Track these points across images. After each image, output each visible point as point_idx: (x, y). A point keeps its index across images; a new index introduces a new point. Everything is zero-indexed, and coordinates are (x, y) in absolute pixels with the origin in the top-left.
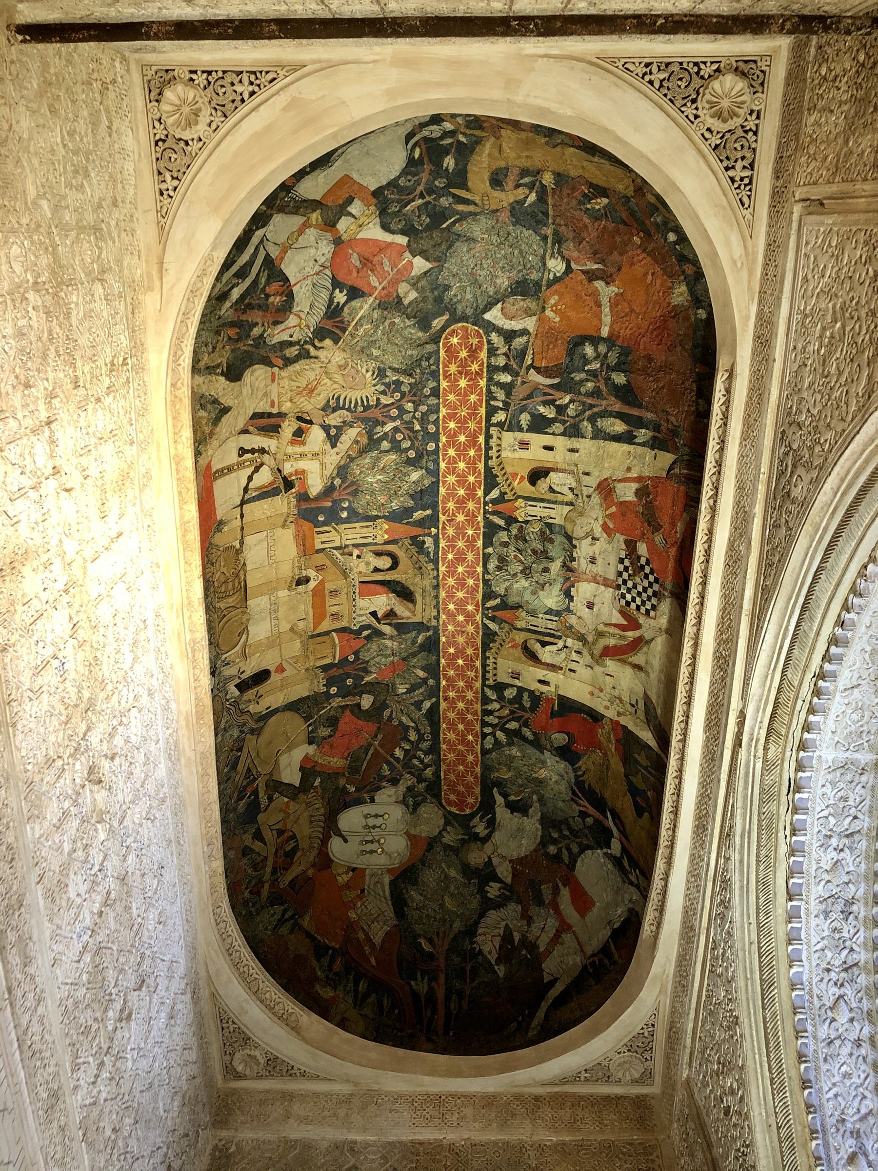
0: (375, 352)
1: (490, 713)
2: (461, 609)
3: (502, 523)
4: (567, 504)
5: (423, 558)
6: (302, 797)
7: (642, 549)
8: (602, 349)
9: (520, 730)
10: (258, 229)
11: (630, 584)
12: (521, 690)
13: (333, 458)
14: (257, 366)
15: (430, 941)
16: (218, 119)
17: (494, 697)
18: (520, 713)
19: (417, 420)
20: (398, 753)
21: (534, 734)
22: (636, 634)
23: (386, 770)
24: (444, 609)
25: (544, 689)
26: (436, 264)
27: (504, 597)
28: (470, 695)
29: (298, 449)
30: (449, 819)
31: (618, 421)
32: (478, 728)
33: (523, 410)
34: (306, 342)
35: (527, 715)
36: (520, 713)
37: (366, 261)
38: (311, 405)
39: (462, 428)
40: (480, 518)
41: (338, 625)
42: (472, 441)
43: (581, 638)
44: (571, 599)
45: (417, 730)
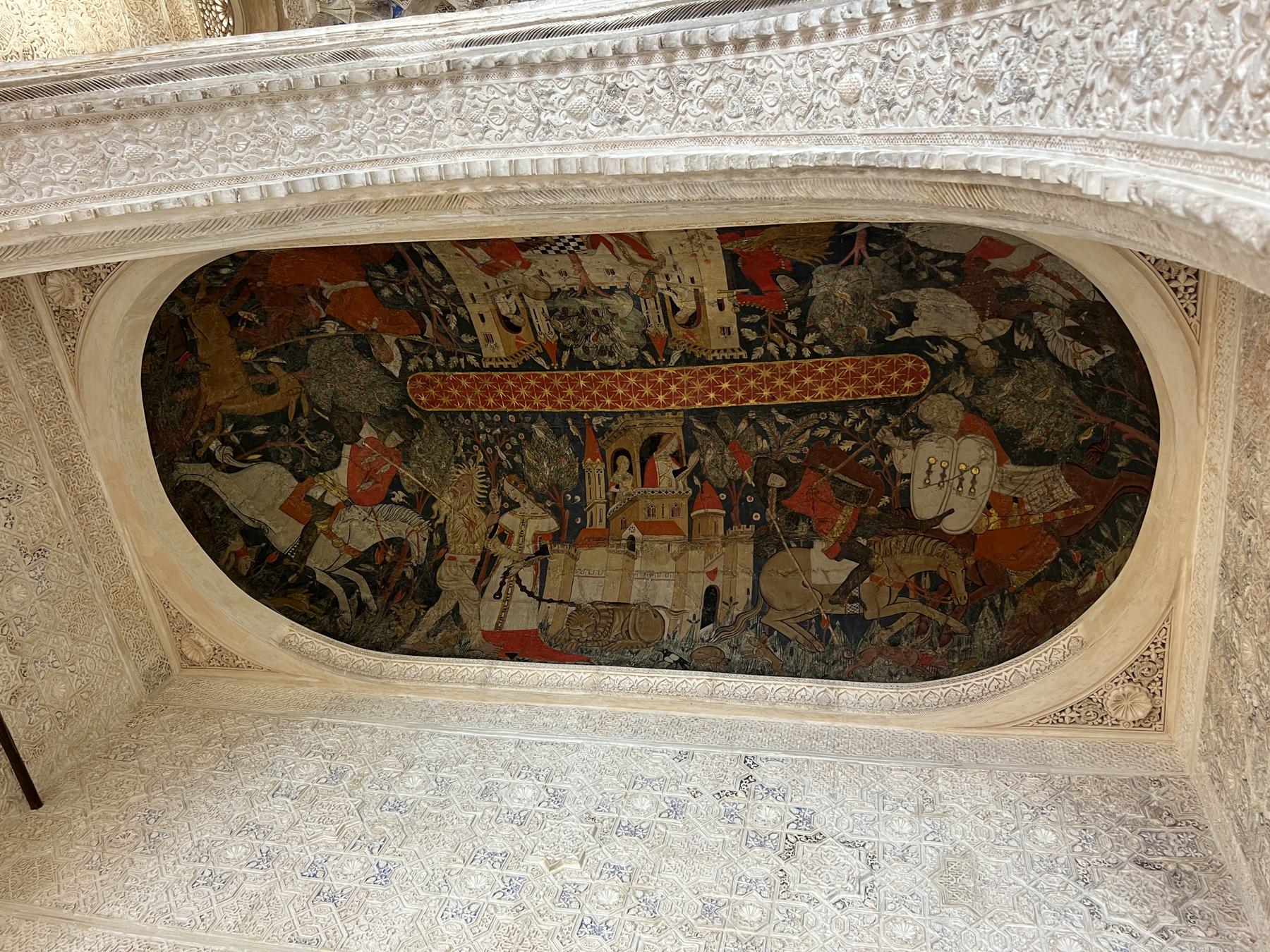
2: (664, 388)
3: (566, 354)
5: (614, 426)
9: (793, 321)
10: (314, 579)
12: (741, 325)
13: (528, 506)
15: (1083, 429)
17: (761, 349)
20: (847, 446)
21: (791, 307)
26: (363, 419)
28: (766, 373)
30: (939, 386)
32: (808, 362)
34: (432, 527)
37: (368, 477)
38: (482, 526)
39: (492, 391)
42: (501, 383)
43: (650, 275)
45: (814, 428)
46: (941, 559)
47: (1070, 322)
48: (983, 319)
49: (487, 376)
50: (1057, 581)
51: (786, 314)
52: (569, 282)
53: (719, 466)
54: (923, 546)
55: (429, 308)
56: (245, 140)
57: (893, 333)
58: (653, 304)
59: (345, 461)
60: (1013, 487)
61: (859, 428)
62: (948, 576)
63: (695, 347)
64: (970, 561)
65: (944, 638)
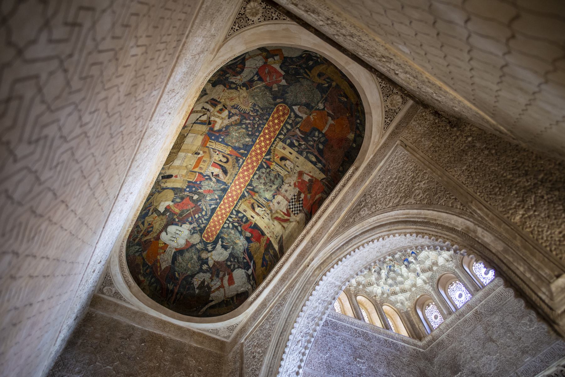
0: (256, 98)
1: (231, 218)
2: (239, 185)
3: (265, 166)
5: (237, 165)
6: (161, 216)
7: (302, 196)
8: (320, 135)
11: (294, 203)
12: (244, 216)
13: (226, 122)
16: (262, 19)
17: (235, 214)
18: (241, 222)
20: (197, 216)
21: (241, 230)
22: (288, 218)
23: (190, 219)
27: (254, 187)
28: (228, 210)
29: (218, 114)
30: (202, 241)
31: (314, 157)
32: (225, 220)
33: (289, 138)
34: (239, 85)
35: (242, 223)
36: (240, 222)
37: (269, 73)
38: (229, 103)
39: (269, 134)
41: (200, 171)
43: (271, 211)
44: (274, 198)
45: (206, 212)
47: (206, 283)
48: (214, 261)
49: (274, 137)
53: (208, 185)
55: (304, 141)
59: (280, 70)
61: (200, 221)
64: (152, 240)
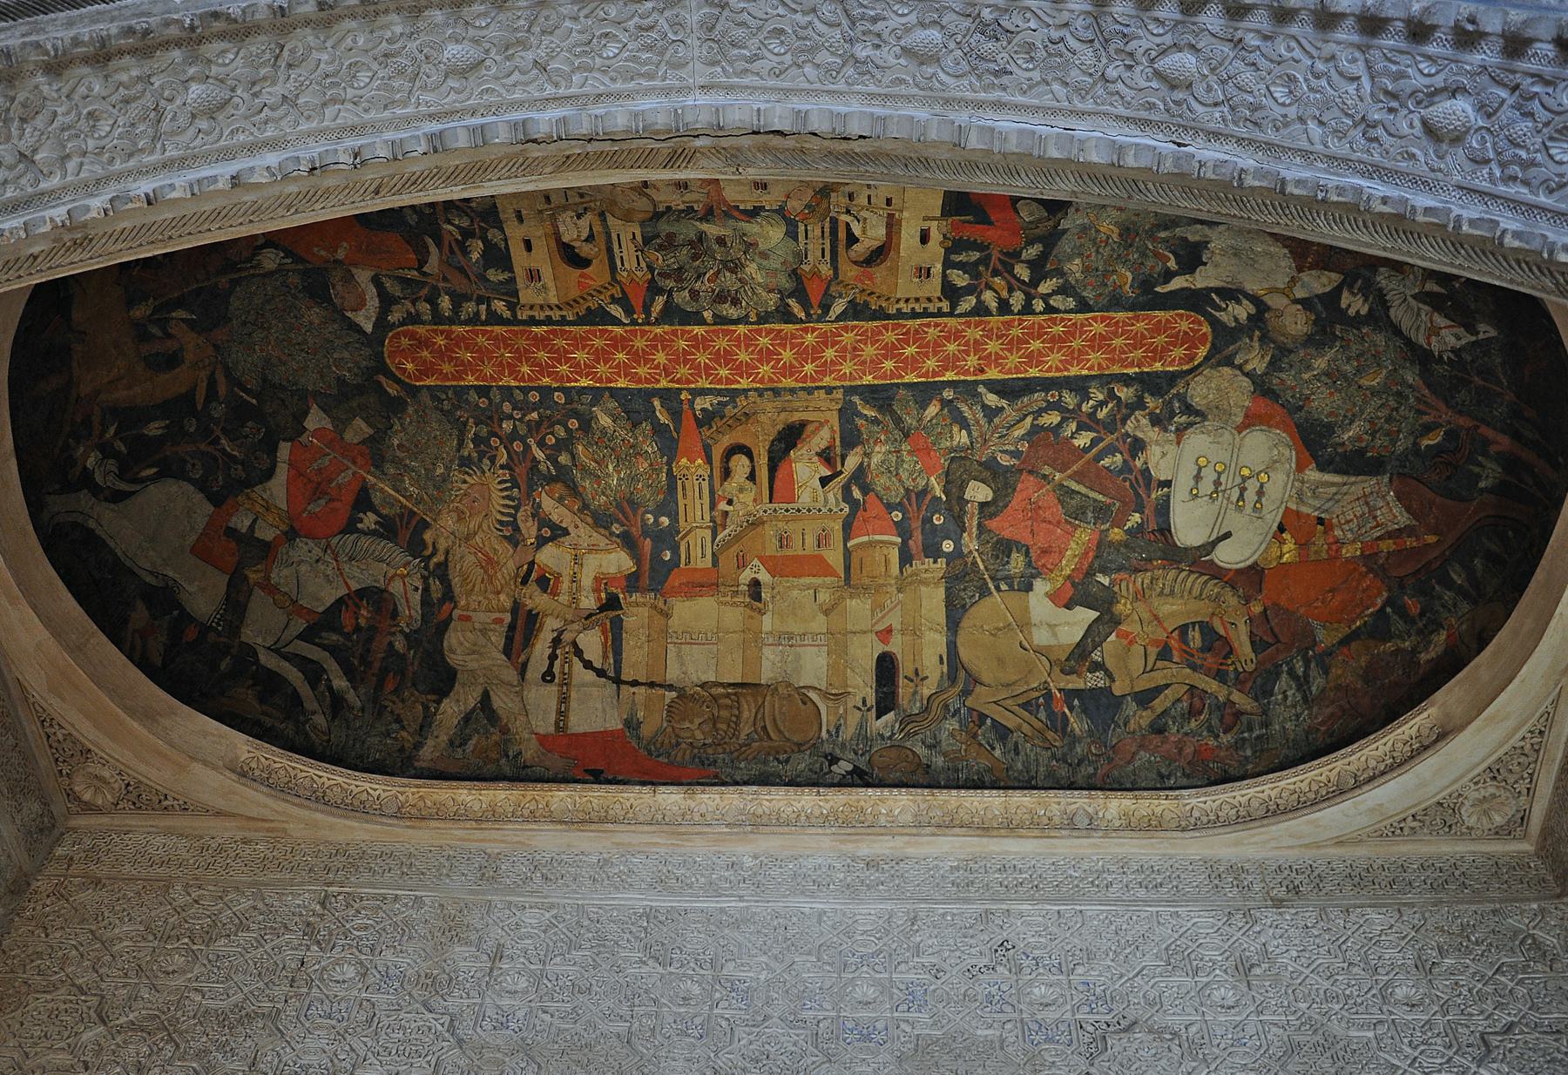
0: (440, 471)
2: (814, 353)
3: (660, 301)
4: (604, 220)
6: (1121, 608)
9: (1028, 262)
12: (947, 264)
13: (583, 533)
14: (445, 644)
19: (524, 415)
20: (1083, 440)
21: (1030, 242)
24: (813, 380)
25: (935, 236)
26: (311, 400)
28: (974, 334)
29: (565, 585)
30: (1221, 355)
34: (426, 568)
37: (318, 491)
38: (509, 562)
40: (658, 330)
41: (838, 535)
42: (541, 342)
45: (1039, 413)
46: (1215, 605)
48: (1300, 269)
50: (1384, 641)
51: (1020, 253)
52: (688, 197)
54: (1189, 584)
56: (369, 69)
57: (1167, 282)
58: (818, 232)
59: (282, 472)
60: (1317, 503)
62: (1225, 628)
63: (872, 293)
64: (1257, 609)
65: (1228, 719)
